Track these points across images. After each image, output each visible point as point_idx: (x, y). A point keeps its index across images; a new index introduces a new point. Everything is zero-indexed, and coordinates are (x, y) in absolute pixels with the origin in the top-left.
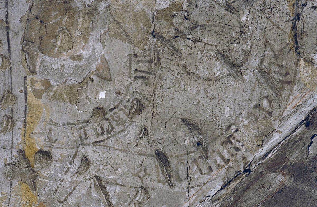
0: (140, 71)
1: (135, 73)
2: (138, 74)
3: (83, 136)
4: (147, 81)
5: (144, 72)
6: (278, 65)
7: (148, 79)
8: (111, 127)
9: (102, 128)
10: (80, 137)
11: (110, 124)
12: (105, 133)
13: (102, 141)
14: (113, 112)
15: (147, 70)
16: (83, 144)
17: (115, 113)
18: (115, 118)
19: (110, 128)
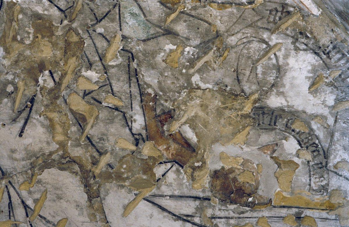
0: (271, 122)
1: (272, 126)
2: (273, 124)
3: (320, 166)
4: (278, 117)
5: (271, 119)
6: (269, 17)
7: (276, 116)
8: (313, 144)
9: (314, 151)
10: (321, 168)
11: (310, 145)
12: (318, 149)
13: (324, 152)
14: (301, 143)
15: (270, 117)
16: (326, 167)
17: (303, 141)
18: (306, 141)
19: (315, 145)
